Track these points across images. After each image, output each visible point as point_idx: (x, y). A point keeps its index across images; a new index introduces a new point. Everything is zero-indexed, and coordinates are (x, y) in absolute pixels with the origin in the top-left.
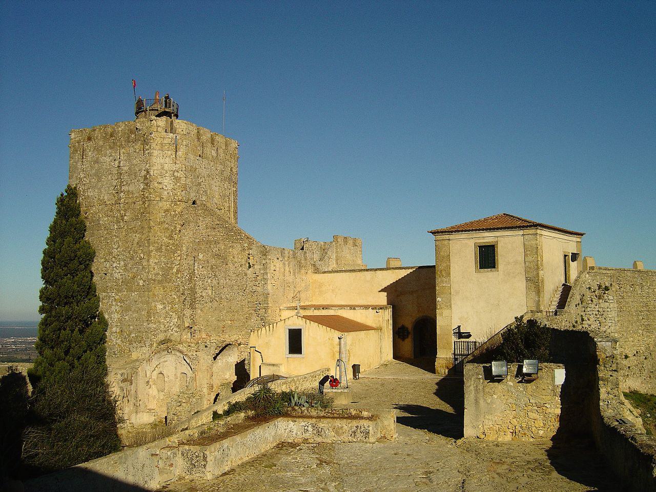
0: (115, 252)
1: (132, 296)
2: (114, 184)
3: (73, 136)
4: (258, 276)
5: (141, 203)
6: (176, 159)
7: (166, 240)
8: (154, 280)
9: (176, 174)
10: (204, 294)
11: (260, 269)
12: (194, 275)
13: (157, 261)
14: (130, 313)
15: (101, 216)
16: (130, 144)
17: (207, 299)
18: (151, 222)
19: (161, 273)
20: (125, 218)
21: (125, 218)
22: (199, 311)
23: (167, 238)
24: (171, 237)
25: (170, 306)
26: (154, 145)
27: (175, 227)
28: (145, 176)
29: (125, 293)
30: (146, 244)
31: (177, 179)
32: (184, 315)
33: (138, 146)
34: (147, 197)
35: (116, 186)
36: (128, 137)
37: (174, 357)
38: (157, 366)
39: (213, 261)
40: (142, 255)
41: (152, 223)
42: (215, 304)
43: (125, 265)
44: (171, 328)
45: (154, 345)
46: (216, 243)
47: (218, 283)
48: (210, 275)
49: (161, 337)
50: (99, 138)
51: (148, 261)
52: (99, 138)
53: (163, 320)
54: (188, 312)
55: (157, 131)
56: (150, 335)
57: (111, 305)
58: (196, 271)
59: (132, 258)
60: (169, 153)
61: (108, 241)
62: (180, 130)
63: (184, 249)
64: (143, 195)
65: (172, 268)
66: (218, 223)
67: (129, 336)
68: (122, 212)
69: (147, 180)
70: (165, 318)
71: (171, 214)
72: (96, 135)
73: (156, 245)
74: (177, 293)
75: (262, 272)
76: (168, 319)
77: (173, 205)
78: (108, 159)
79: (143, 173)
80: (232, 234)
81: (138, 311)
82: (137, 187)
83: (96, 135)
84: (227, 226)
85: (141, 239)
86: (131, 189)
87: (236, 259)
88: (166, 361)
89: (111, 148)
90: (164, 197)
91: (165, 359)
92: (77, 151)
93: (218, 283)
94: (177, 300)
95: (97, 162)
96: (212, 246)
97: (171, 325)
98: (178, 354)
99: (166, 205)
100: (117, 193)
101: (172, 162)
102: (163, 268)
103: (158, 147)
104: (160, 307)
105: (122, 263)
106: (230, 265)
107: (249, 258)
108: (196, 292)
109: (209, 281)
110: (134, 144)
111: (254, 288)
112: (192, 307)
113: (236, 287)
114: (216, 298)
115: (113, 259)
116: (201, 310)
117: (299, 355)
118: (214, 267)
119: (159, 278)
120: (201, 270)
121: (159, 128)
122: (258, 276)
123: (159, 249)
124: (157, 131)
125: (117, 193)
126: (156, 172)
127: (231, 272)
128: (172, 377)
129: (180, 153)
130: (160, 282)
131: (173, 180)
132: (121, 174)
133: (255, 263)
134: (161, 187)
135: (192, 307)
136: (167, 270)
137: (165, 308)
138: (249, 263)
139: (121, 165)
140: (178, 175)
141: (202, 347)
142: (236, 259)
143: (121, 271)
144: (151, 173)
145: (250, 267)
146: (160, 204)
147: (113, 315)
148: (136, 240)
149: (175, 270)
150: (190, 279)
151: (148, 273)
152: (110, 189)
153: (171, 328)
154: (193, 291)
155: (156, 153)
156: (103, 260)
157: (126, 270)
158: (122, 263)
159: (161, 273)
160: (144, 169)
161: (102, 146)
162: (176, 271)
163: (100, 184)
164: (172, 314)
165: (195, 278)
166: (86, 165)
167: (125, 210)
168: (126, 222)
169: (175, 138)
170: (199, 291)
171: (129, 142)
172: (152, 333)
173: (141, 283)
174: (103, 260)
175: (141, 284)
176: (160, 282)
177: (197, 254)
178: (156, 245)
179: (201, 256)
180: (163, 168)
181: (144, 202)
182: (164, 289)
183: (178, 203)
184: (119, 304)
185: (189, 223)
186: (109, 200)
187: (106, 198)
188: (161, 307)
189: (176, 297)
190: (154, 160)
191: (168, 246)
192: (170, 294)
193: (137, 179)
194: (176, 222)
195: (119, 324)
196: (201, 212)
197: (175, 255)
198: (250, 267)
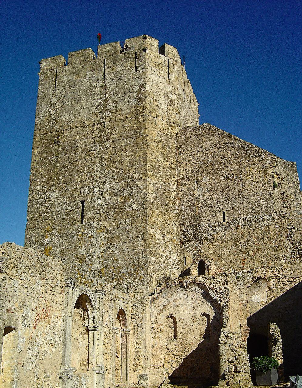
0: (97, 175)
1: (121, 223)
2: (97, 103)
3: (43, 64)
4: (288, 196)
5: (134, 119)
7: (162, 161)
8: (152, 204)
9: (169, 95)
10: (213, 222)
11: (289, 188)
13: (155, 182)
14: (119, 244)
15: (78, 138)
16: (117, 63)
17: (217, 228)
18: (148, 139)
21: (112, 136)
22: (207, 243)
23: (164, 158)
25: (169, 236)
26: (148, 62)
27: (172, 149)
28: (139, 93)
29: (112, 221)
30: (142, 163)
31: (172, 101)
32: (185, 249)
33: (129, 63)
34: (142, 112)
35: (98, 105)
36: (115, 57)
37: (191, 294)
38: (164, 307)
39: (224, 184)
40: (136, 175)
41: (149, 140)
42: (230, 233)
43: (112, 188)
44: (171, 264)
45: (153, 283)
47: (233, 208)
49: (161, 273)
50: (77, 62)
51: (145, 181)
52: (77, 62)
53: (162, 253)
54: (191, 245)
55: (151, 49)
56: (149, 270)
57: (90, 238)
59: (122, 179)
60: (163, 73)
61: (88, 164)
62: (172, 55)
64: (136, 110)
65: (170, 194)
66: (228, 141)
67: (117, 272)
68: (107, 131)
69: (141, 94)
71: (167, 135)
72: (73, 60)
73: (153, 164)
75: (293, 191)
77: (168, 125)
78: (88, 81)
79: (136, 88)
80: (248, 152)
81: (132, 240)
82: (126, 104)
83: (73, 60)
84: (240, 144)
85: (133, 157)
86: (119, 106)
87: (255, 179)
88: (179, 300)
89: (92, 69)
90: (160, 115)
91: (178, 297)
92: (48, 77)
95: (74, 84)
96: (221, 167)
98: (197, 288)
99: (162, 124)
100: (100, 112)
101: (165, 83)
103: (153, 64)
104: (159, 236)
105: (107, 187)
106: (249, 186)
107: (273, 177)
108: (202, 221)
110: (123, 62)
111: (284, 210)
112: (197, 238)
115: (95, 183)
116: (210, 242)
118: (225, 190)
119: (157, 202)
121: (152, 47)
122: (288, 196)
123: (156, 169)
124: (151, 49)
125: (100, 112)
126: (151, 87)
128: (188, 321)
130: (157, 207)
131: (168, 101)
132: (105, 93)
134: (156, 104)
135: (197, 238)
136: (165, 193)
138: (274, 182)
139: (106, 84)
140: (172, 97)
141: (231, 278)
142: (255, 179)
143: (106, 196)
144: (147, 87)
145: (275, 186)
146: (157, 122)
147: (93, 250)
148: (128, 159)
150: (193, 207)
151: (146, 194)
152: (91, 109)
154: (197, 219)
155: (150, 69)
156: (80, 186)
157: (113, 193)
158: (107, 187)
160: (137, 84)
161: (80, 70)
162: (173, 197)
163: (77, 106)
164: (171, 247)
166: (60, 89)
167: (112, 129)
168: (112, 141)
170: (206, 219)
171: (116, 61)
173: (135, 207)
174: (80, 186)
175: (135, 208)
177: (201, 178)
178: (153, 164)
179: (206, 179)
180: (157, 86)
181: (138, 118)
183: (173, 125)
184: (102, 235)
185: (188, 145)
186: (89, 121)
187: (85, 119)
188: (160, 236)
190: (149, 76)
191: (165, 168)
192: (169, 223)
193: (128, 95)
194: (172, 144)
195: (102, 259)
196: (203, 132)
197: (172, 179)
198: (275, 186)
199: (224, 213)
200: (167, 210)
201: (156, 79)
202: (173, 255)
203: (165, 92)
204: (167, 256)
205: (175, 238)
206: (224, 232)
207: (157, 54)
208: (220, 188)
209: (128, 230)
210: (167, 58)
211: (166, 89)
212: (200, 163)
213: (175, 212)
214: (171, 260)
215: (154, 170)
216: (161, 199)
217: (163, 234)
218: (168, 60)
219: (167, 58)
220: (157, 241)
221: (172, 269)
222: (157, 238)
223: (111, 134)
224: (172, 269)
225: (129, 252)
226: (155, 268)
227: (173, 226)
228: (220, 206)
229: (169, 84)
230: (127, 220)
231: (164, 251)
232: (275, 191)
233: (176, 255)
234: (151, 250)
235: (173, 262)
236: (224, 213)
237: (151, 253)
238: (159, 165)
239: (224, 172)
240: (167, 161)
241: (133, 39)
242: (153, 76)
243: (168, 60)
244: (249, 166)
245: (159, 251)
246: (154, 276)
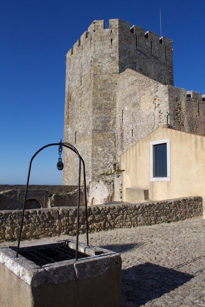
5: (90, 78)
6: (112, 45)
8: (96, 130)
10: (128, 137)
12: (122, 123)
19: (101, 125)
20: (84, 92)
24: (109, 99)
44: (109, 165)
46: (135, 94)
47: (136, 126)
48: (131, 121)
53: (102, 159)
58: (124, 121)
60: (107, 41)
62: (114, 26)
63: (118, 106)
65: (109, 121)
70: (104, 158)
73: (98, 105)
74: (114, 139)
76: (106, 159)
80: (144, 84)
90: (103, 71)
93: (136, 126)
94: (113, 144)
97: (108, 163)
102: (103, 121)
104: (100, 149)
109: (131, 126)
113: (147, 127)
114: (135, 139)
117: (152, 176)
119: (100, 128)
120: (127, 118)
121: (99, 27)
127: (144, 115)
129: (114, 41)
130: (100, 131)
133: (159, 103)
137: (104, 150)
149: (111, 122)
153: (109, 165)
159: (101, 125)
160: (91, 56)
162: (112, 123)
164: (109, 154)
165: (123, 126)
169: (110, 31)
170: (125, 134)
172: (94, 168)
174: (75, 123)
175: (89, 134)
176: (100, 131)
178: (98, 105)
179: (126, 108)
181: (91, 78)
182: (103, 136)
189: (112, 142)
191: (106, 105)
192: (108, 140)
196: (125, 75)
197: (112, 111)
199: (132, 130)
200: (107, 132)
201: (101, 48)
202: (110, 160)
203: (108, 55)
204: (106, 161)
205: (113, 149)
206: (132, 143)
207: (102, 30)
208: (131, 113)
209: (87, 147)
210: (111, 30)
211: (108, 53)
212: (124, 97)
213: (113, 132)
214: (108, 163)
215: (98, 109)
216: (102, 127)
217: (103, 147)
218: (111, 30)
219: (110, 30)
220: (99, 153)
221: (109, 169)
222: (99, 151)
223: (84, 91)
224: (109, 169)
225: (87, 160)
226: (96, 169)
227: (112, 141)
228: (131, 126)
229: (111, 47)
230: (87, 141)
231: (104, 158)
232: (156, 111)
233: (112, 159)
234: (94, 158)
235: (110, 164)
236: (132, 130)
237: (95, 160)
238: (102, 105)
239: (133, 101)
240: (108, 100)
241: (90, 26)
242: (99, 47)
243: (111, 30)
244: (144, 94)
245: (99, 158)
246: (96, 174)
